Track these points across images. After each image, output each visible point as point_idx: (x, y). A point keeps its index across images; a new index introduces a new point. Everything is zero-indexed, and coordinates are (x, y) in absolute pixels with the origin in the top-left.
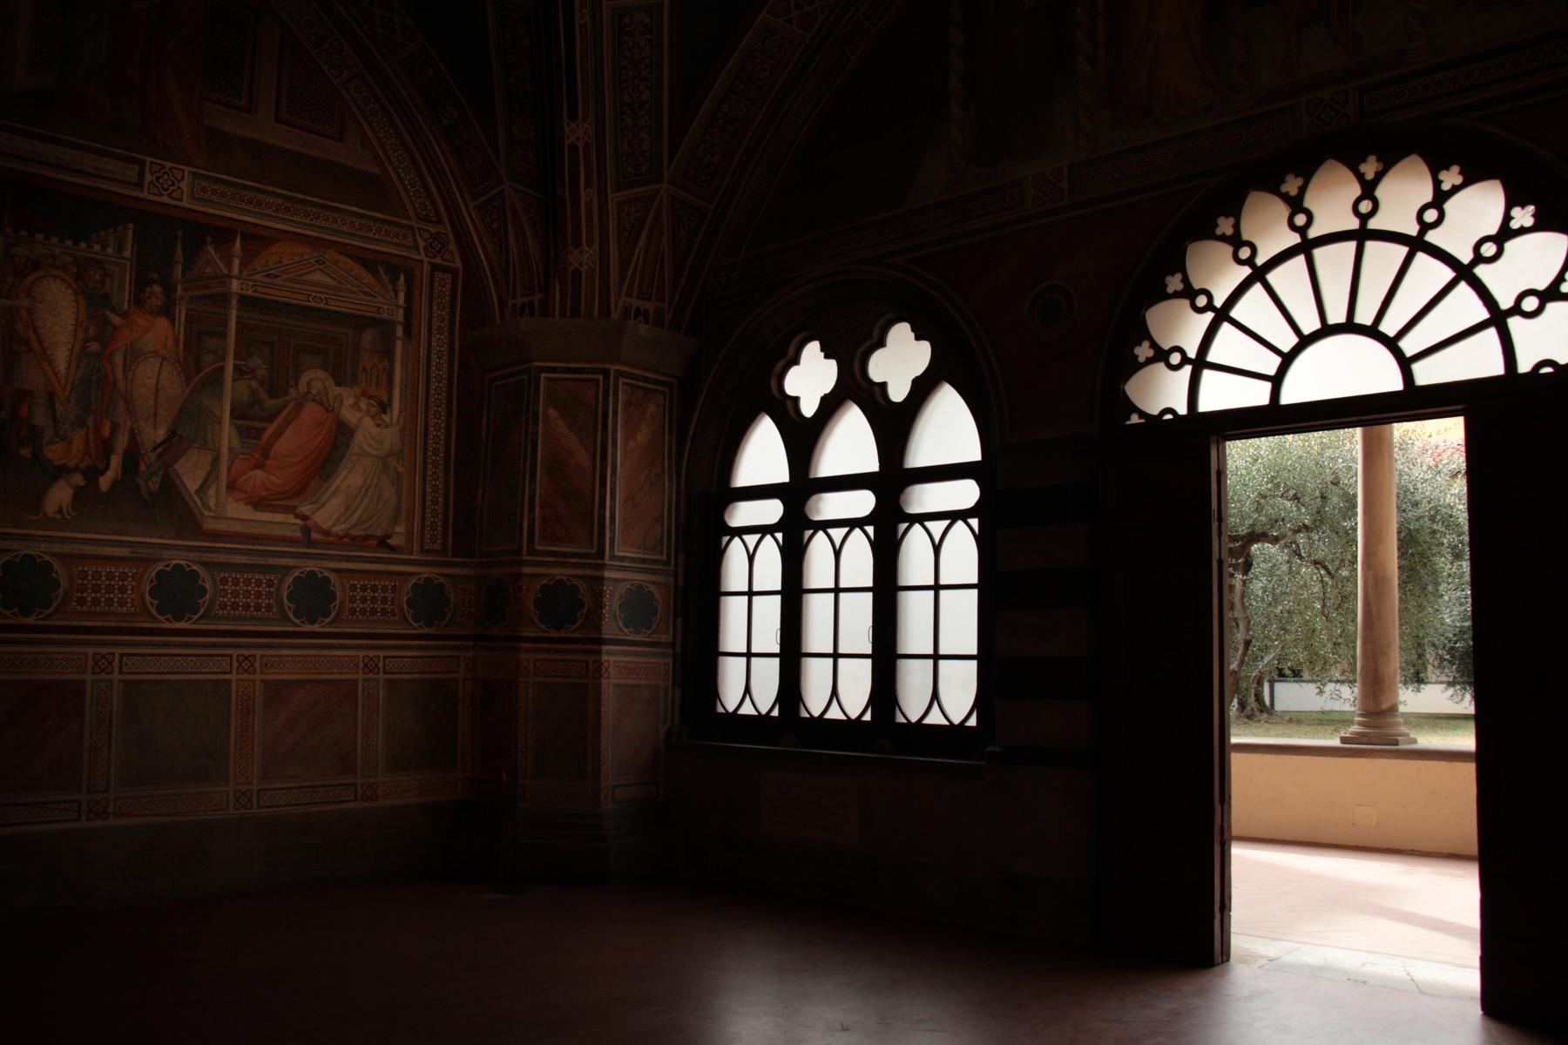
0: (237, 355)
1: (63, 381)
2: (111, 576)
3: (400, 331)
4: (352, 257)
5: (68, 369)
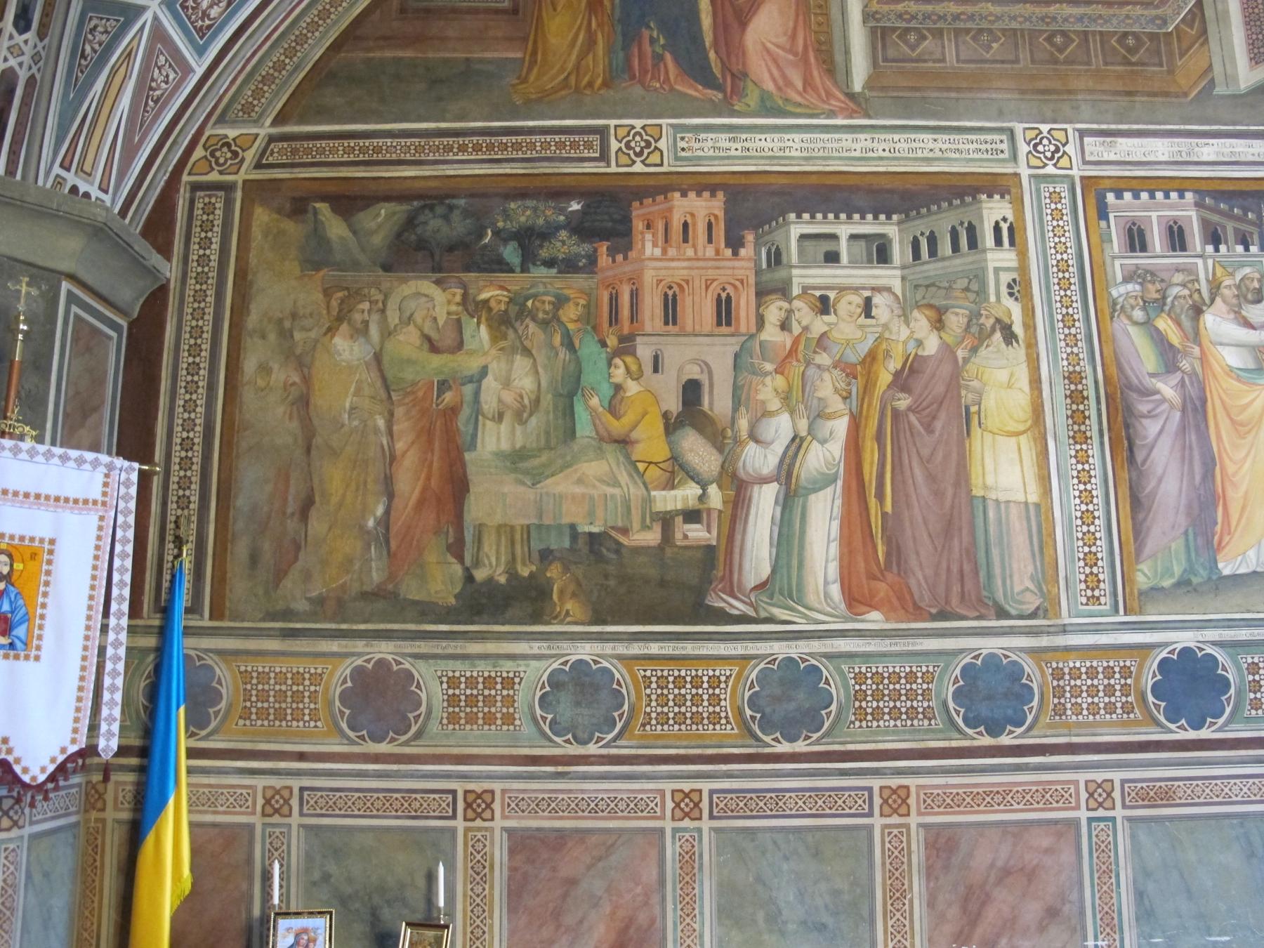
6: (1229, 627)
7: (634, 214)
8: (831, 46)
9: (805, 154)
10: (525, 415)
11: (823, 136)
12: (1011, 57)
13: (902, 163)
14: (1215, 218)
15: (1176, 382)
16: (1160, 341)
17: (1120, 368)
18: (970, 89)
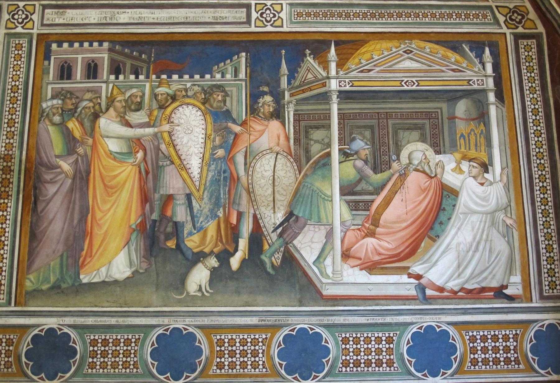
0: (341, 141)
1: (197, 183)
2: (244, 343)
3: (492, 97)
4: (437, 43)
5: (201, 173)
6: (81, 316)
14: (120, 58)
16: (68, 136)
17: (38, 152)
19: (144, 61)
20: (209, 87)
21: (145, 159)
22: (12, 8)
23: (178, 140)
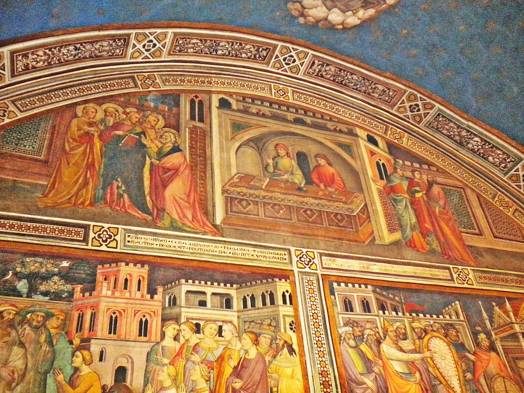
7: (98, 271)
8: (207, 202)
9: (191, 251)
10: (14, 384)
11: (200, 243)
12: (289, 217)
13: (239, 260)
14: (382, 298)
15: (373, 377)
18: (270, 229)
19: (398, 302)
20: (445, 325)
21: (422, 379)
22: (298, 253)
23: (439, 365)
